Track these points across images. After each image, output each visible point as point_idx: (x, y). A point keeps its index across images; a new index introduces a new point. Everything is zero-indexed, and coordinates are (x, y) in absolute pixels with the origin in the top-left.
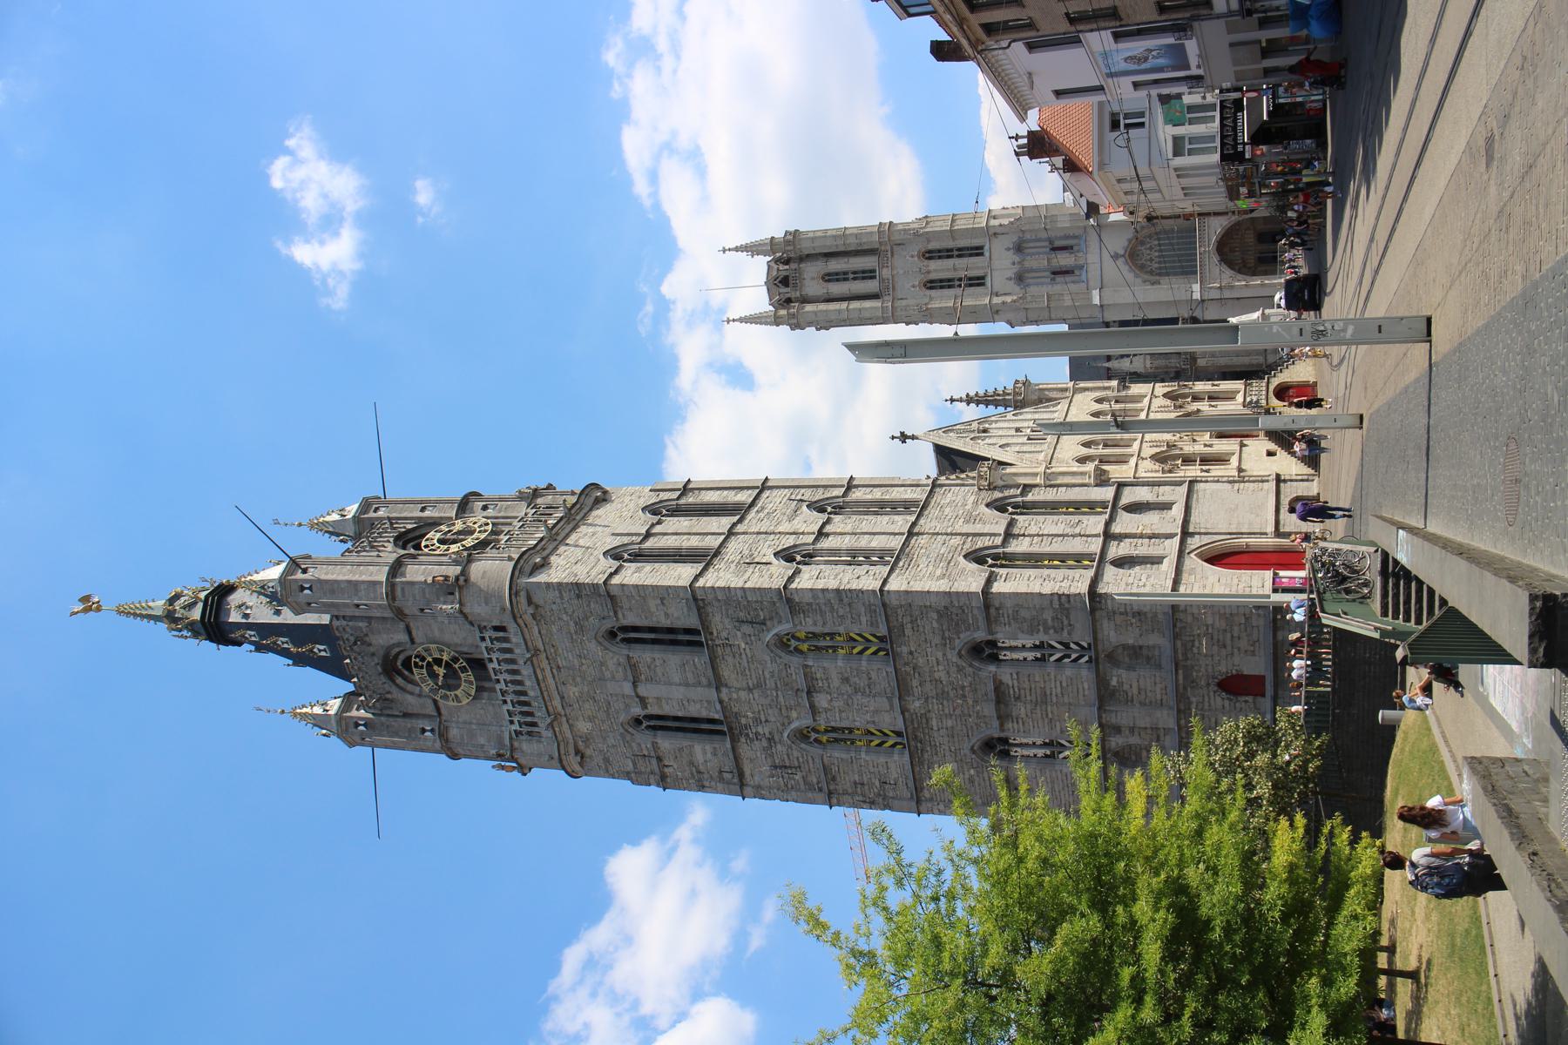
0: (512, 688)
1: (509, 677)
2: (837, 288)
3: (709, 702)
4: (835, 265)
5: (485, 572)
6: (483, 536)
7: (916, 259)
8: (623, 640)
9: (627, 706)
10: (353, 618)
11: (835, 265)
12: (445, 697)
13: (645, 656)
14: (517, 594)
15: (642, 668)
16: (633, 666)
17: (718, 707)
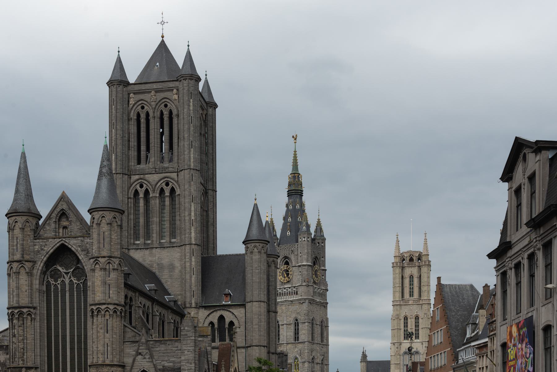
0: (284, 293)
1: (286, 292)
2: (407, 281)
3: (283, 340)
4: (416, 281)
5: (309, 291)
6: (317, 282)
7: (416, 314)
8: (295, 323)
9: (281, 321)
10: (298, 250)
11: (416, 281)
12: (280, 272)
13: (292, 327)
14: (305, 300)
15: (290, 326)
16: (290, 324)
17: (282, 343)
